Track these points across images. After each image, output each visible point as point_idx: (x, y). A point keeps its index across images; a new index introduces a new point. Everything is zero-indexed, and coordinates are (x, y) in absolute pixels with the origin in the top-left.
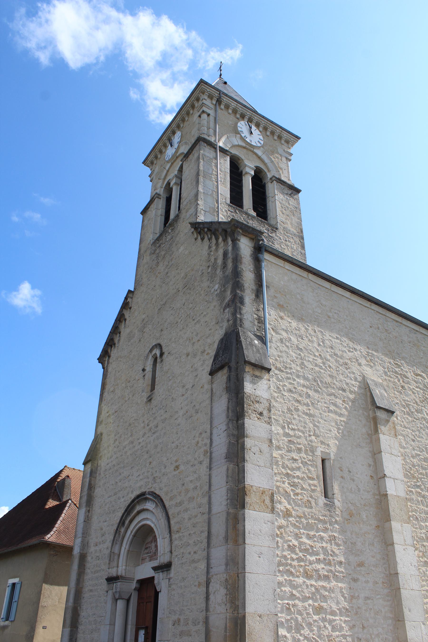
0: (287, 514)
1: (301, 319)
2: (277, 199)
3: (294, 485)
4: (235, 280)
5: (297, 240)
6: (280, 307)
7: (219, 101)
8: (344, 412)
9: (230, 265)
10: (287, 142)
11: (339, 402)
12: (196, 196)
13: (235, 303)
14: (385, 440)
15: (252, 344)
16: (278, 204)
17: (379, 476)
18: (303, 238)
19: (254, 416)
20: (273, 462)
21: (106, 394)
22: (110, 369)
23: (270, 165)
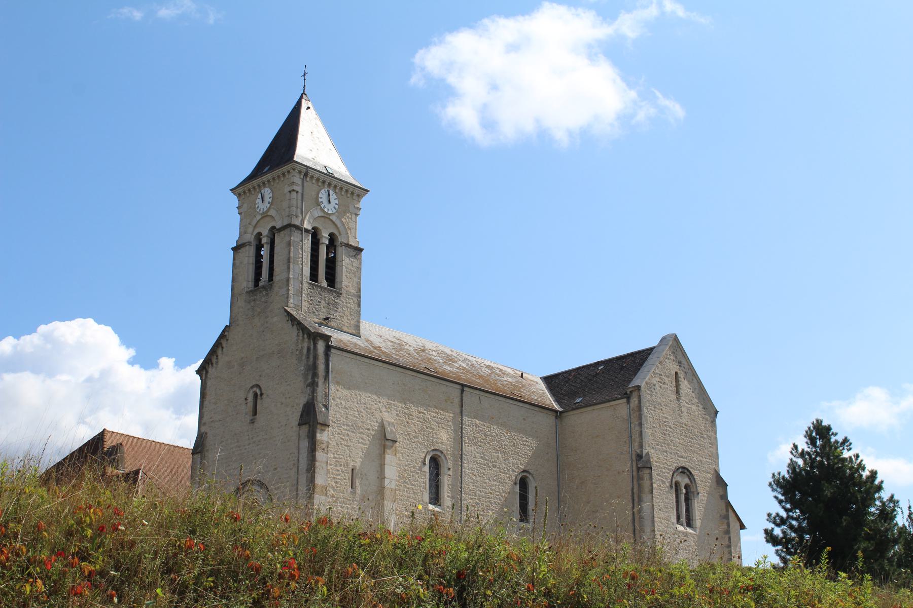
0: (332, 496)
1: (349, 389)
2: (345, 262)
3: (337, 483)
4: (313, 369)
5: (355, 300)
6: (338, 383)
7: (306, 175)
8: (368, 443)
9: (311, 359)
10: (358, 196)
11: (365, 437)
12: (288, 280)
13: (313, 385)
14: (389, 457)
15: (321, 412)
16: (344, 269)
17: (382, 477)
18: (359, 297)
19: (320, 451)
20: (328, 472)
21: (206, 403)
22: (209, 383)
23: (341, 229)
